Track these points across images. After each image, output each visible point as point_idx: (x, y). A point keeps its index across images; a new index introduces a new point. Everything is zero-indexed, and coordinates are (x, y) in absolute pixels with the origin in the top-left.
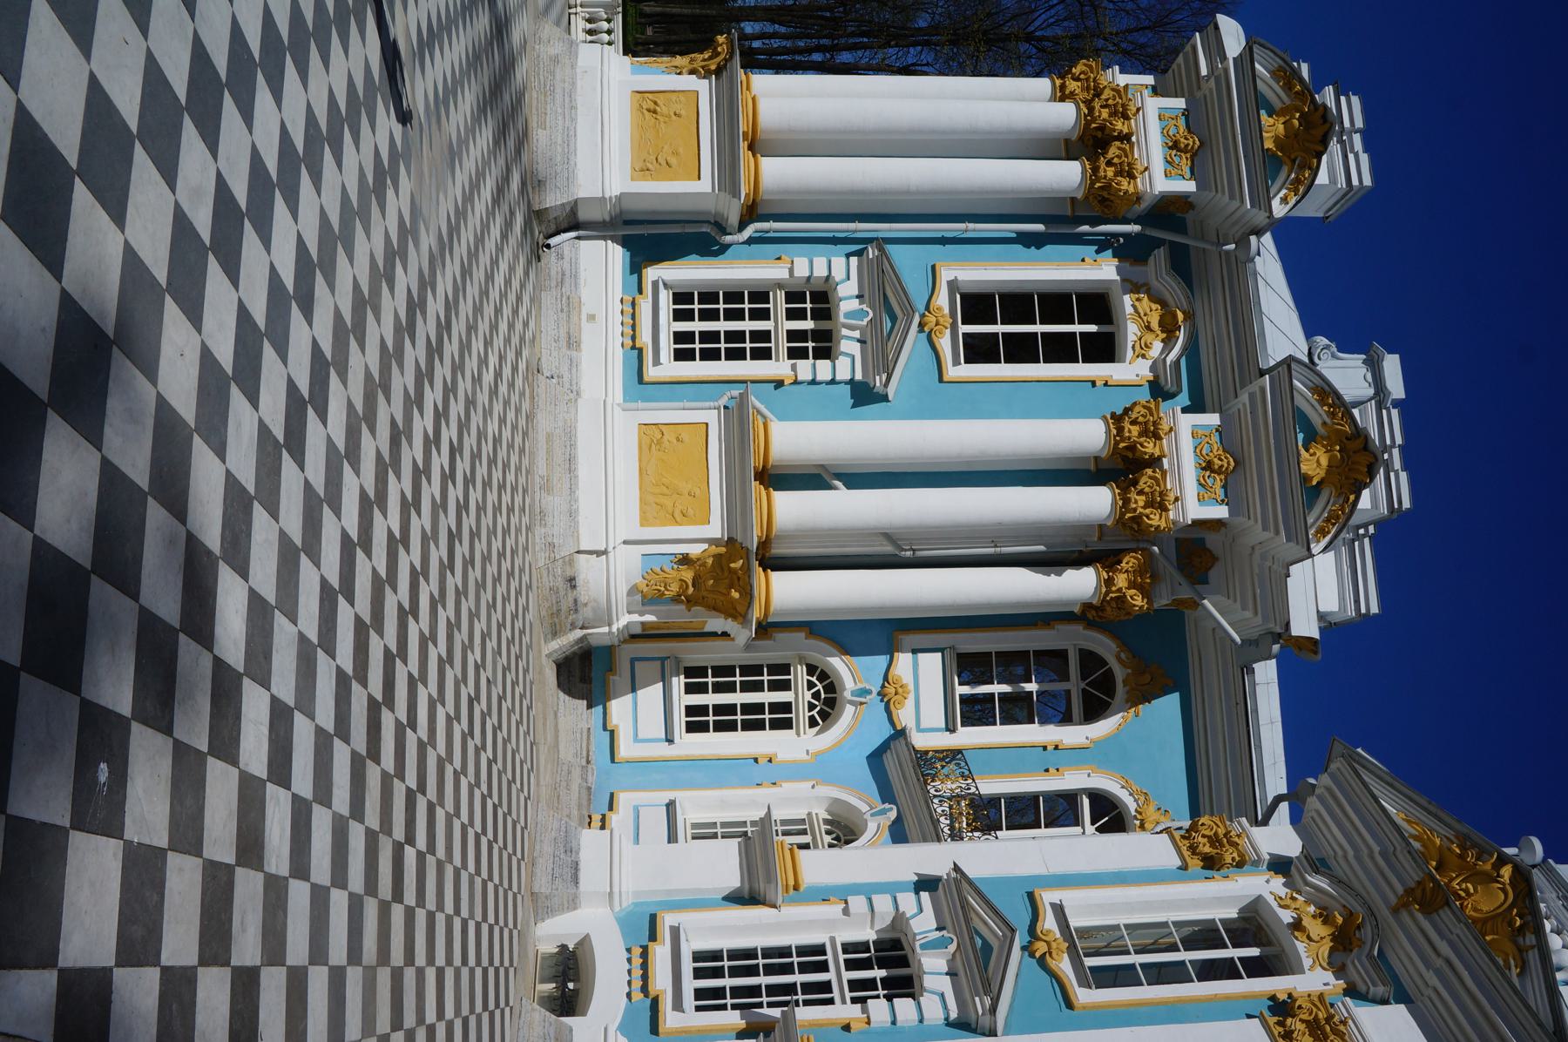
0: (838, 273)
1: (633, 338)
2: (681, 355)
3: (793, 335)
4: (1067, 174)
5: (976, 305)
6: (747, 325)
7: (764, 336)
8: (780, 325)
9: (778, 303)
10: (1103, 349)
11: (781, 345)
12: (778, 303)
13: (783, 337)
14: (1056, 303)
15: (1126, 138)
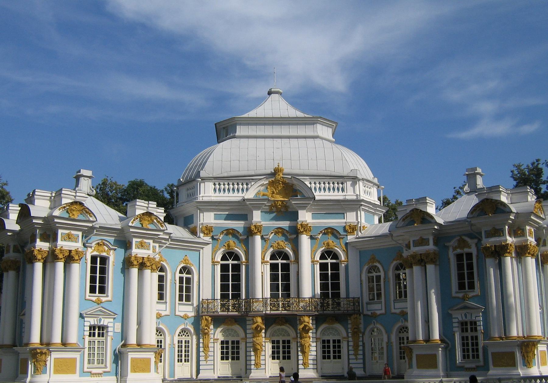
0: (456, 320)
1: (474, 369)
2: (478, 357)
3: (472, 331)
4: (430, 268)
5: (461, 286)
6: (470, 341)
7: (472, 337)
8: (469, 334)
9: (465, 334)
10: (469, 256)
11: (474, 334)
12: (465, 334)
13: (472, 333)
14: (460, 267)
15: (421, 254)
